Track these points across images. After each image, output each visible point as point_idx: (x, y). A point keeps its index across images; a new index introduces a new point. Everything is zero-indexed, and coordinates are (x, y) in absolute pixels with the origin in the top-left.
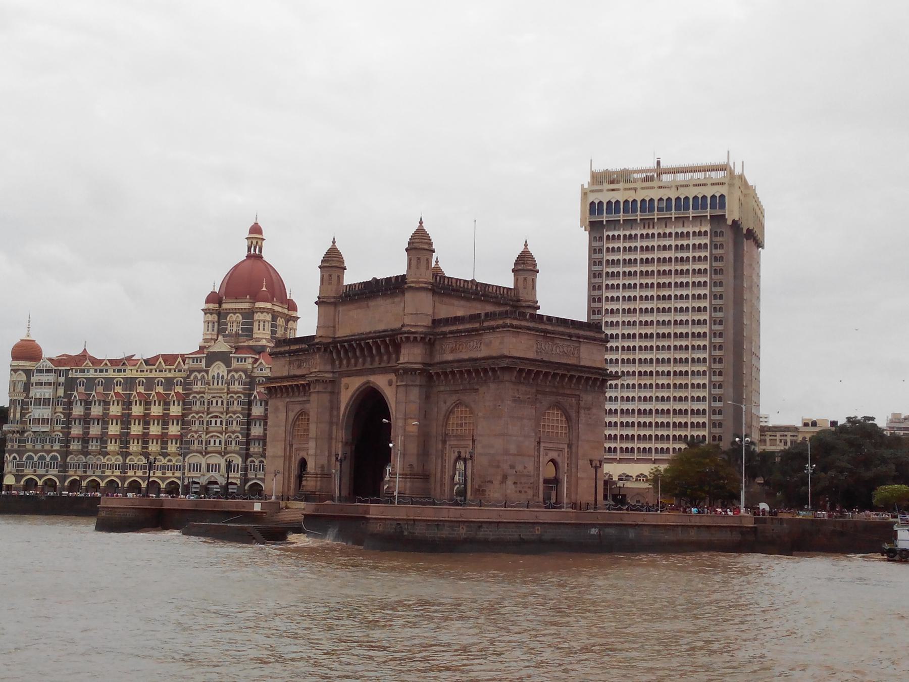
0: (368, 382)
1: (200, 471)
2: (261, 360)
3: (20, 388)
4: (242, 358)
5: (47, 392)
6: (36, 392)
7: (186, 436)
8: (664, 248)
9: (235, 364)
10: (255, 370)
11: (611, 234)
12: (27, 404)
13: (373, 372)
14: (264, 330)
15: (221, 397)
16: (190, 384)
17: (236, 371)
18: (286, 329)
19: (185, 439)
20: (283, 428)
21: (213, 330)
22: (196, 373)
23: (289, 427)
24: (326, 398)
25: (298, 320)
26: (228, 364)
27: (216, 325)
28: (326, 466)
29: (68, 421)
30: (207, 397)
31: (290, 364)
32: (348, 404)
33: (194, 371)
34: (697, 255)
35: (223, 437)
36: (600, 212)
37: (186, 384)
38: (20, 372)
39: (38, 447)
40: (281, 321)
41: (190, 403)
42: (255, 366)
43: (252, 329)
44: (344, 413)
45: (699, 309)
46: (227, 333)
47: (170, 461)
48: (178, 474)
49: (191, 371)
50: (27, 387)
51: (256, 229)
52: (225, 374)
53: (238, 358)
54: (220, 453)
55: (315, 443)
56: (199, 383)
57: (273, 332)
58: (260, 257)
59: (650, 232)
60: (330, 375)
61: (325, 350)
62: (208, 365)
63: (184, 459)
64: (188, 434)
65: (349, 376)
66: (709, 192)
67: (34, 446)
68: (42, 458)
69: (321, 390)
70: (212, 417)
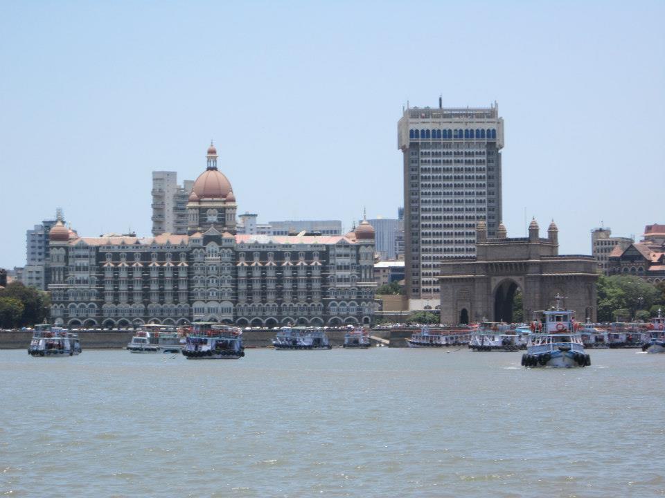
3: (62, 259)
5: (85, 262)
8: (458, 162)
9: (224, 244)
11: (424, 151)
12: (67, 270)
13: (511, 275)
16: (192, 256)
17: (226, 248)
19: (191, 292)
22: (196, 250)
24: (485, 285)
29: (101, 281)
33: (194, 248)
34: (479, 167)
35: (220, 291)
36: (417, 137)
37: (189, 257)
38: (62, 249)
39: (79, 298)
43: (224, 220)
45: (481, 201)
46: (207, 222)
48: (187, 314)
49: (193, 248)
50: (66, 258)
51: (212, 152)
52: (218, 250)
54: (218, 301)
56: (199, 255)
59: (449, 151)
60: (487, 276)
63: (191, 305)
64: (193, 289)
65: (496, 275)
66: (486, 127)
67: (75, 299)
68: (81, 306)
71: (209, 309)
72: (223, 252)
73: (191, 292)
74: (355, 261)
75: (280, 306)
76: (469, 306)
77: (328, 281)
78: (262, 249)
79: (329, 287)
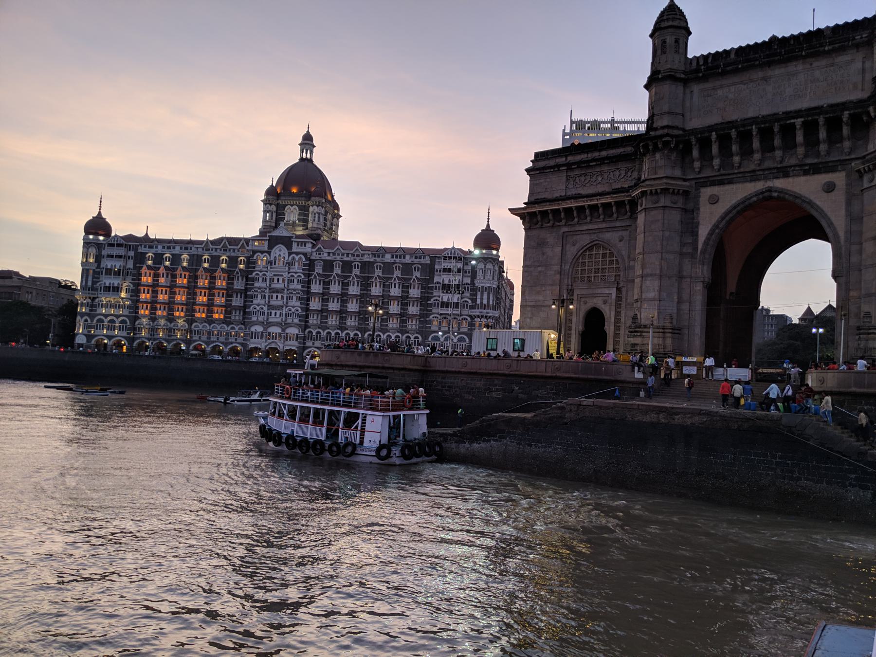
0: (770, 190)
1: (261, 338)
2: (320, 245)
4: (302, 242)
5: (117, 264)
6: (108, 263)
7: (249, 308)
9: (295, 248)
10: (314, 254)
12: (98, 273)
13: (784, 173)
14: (319, 221)
15: (282, 276)
17: (297, 254)
18: (332, 224)
20: (557, 268)
21: (272, 219)
22: (259, 254)
23: (567, 267)
24: (675, 217)
25: (340, 219)
26: (289, 246)
27: (274, 215)
28: (675, 316)
30: (269, 275)
31: (567, 180)
32: (716, 226)
37: (250, 263)
40: (329, 217)
41: (253, 279)
42: (314, 250)
44: (708, 239)
47: (233, 328)
50: (98, 259)
52: (286, 256)
53: (298, 243)
55: (656, 283)
57: (325, 225)
58: (311, 160)
61: (677, 145)
62: (271, 247)
64: (251, 305)
65: (721, 183)
69: (668, 204)
70: (273, 292)
71: (269, 333)
72: (294, 258)
73: (247, 310)
74: (469, 281)
75: (363, 336)
76: (614, 296)
77: (431, 305)
78: (346, 259)
79: (431, 314)
